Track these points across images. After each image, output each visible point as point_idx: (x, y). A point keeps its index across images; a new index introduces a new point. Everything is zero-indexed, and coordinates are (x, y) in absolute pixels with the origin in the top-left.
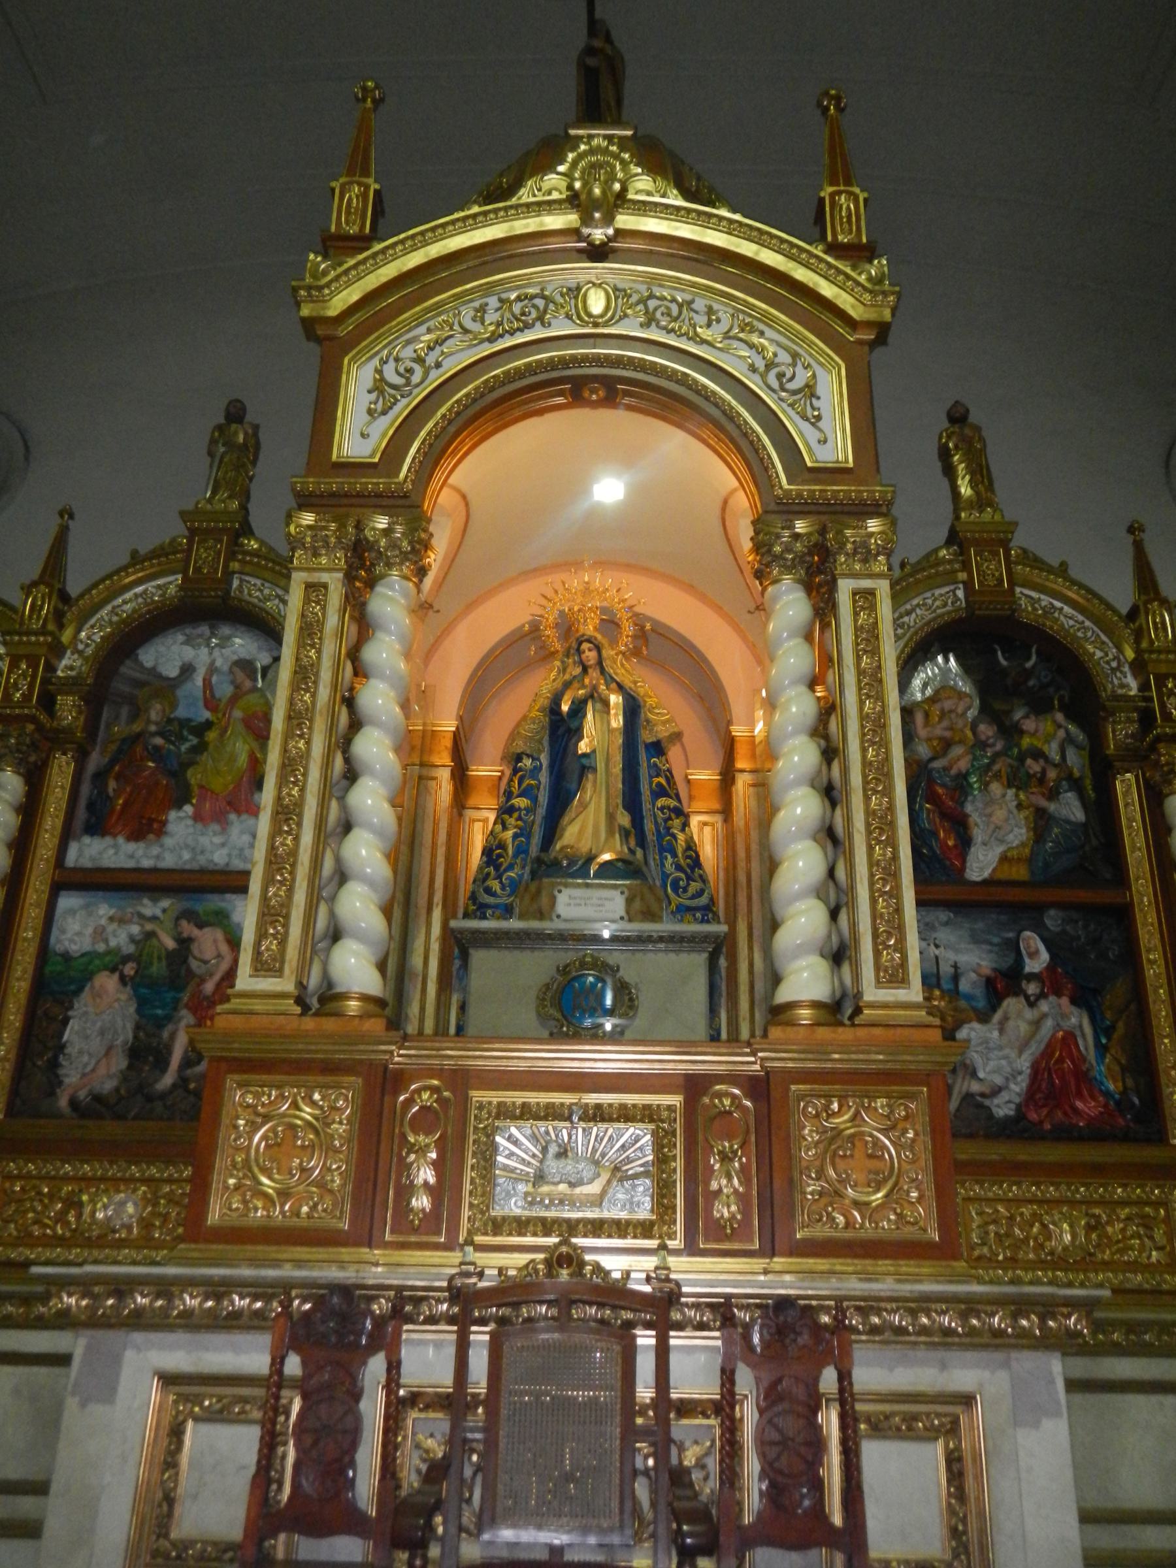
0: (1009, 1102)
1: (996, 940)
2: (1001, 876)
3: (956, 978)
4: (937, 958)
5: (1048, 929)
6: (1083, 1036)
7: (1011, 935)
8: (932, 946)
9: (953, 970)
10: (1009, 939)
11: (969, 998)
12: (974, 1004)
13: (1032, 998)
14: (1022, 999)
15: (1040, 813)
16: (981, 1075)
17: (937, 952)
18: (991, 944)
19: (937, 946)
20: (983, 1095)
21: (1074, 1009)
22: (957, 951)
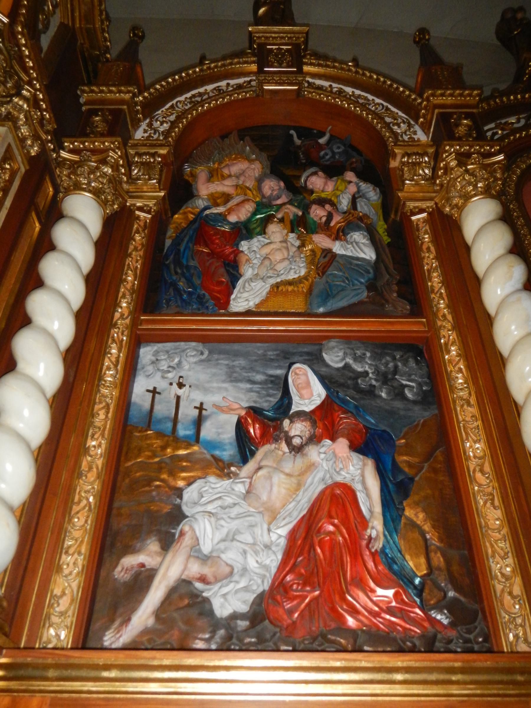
0: (246, 589)
1: (259, 377)
2: (271, 307)
3: (199, 422)
4: (178, 398)
5: (327, 366)
6: (366, 488)
7: (280, 372)
8: (175, 386)
9: (197, 411)
10: (277, 377)
11: (211, 445)
12: (217, 453)
13: (297, 441)
14: (284, 447)
15: (327, 252)
16: (206, 548)
17: (180, 392)
18: (253, 382)
19: (181, 385)
20: (203, 579)
21: (356, 458)
22: (206, 390)
